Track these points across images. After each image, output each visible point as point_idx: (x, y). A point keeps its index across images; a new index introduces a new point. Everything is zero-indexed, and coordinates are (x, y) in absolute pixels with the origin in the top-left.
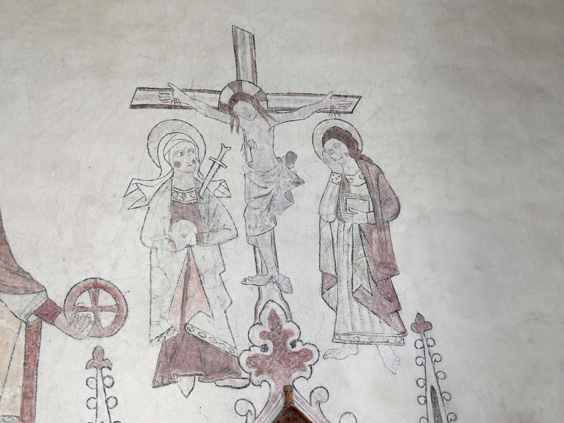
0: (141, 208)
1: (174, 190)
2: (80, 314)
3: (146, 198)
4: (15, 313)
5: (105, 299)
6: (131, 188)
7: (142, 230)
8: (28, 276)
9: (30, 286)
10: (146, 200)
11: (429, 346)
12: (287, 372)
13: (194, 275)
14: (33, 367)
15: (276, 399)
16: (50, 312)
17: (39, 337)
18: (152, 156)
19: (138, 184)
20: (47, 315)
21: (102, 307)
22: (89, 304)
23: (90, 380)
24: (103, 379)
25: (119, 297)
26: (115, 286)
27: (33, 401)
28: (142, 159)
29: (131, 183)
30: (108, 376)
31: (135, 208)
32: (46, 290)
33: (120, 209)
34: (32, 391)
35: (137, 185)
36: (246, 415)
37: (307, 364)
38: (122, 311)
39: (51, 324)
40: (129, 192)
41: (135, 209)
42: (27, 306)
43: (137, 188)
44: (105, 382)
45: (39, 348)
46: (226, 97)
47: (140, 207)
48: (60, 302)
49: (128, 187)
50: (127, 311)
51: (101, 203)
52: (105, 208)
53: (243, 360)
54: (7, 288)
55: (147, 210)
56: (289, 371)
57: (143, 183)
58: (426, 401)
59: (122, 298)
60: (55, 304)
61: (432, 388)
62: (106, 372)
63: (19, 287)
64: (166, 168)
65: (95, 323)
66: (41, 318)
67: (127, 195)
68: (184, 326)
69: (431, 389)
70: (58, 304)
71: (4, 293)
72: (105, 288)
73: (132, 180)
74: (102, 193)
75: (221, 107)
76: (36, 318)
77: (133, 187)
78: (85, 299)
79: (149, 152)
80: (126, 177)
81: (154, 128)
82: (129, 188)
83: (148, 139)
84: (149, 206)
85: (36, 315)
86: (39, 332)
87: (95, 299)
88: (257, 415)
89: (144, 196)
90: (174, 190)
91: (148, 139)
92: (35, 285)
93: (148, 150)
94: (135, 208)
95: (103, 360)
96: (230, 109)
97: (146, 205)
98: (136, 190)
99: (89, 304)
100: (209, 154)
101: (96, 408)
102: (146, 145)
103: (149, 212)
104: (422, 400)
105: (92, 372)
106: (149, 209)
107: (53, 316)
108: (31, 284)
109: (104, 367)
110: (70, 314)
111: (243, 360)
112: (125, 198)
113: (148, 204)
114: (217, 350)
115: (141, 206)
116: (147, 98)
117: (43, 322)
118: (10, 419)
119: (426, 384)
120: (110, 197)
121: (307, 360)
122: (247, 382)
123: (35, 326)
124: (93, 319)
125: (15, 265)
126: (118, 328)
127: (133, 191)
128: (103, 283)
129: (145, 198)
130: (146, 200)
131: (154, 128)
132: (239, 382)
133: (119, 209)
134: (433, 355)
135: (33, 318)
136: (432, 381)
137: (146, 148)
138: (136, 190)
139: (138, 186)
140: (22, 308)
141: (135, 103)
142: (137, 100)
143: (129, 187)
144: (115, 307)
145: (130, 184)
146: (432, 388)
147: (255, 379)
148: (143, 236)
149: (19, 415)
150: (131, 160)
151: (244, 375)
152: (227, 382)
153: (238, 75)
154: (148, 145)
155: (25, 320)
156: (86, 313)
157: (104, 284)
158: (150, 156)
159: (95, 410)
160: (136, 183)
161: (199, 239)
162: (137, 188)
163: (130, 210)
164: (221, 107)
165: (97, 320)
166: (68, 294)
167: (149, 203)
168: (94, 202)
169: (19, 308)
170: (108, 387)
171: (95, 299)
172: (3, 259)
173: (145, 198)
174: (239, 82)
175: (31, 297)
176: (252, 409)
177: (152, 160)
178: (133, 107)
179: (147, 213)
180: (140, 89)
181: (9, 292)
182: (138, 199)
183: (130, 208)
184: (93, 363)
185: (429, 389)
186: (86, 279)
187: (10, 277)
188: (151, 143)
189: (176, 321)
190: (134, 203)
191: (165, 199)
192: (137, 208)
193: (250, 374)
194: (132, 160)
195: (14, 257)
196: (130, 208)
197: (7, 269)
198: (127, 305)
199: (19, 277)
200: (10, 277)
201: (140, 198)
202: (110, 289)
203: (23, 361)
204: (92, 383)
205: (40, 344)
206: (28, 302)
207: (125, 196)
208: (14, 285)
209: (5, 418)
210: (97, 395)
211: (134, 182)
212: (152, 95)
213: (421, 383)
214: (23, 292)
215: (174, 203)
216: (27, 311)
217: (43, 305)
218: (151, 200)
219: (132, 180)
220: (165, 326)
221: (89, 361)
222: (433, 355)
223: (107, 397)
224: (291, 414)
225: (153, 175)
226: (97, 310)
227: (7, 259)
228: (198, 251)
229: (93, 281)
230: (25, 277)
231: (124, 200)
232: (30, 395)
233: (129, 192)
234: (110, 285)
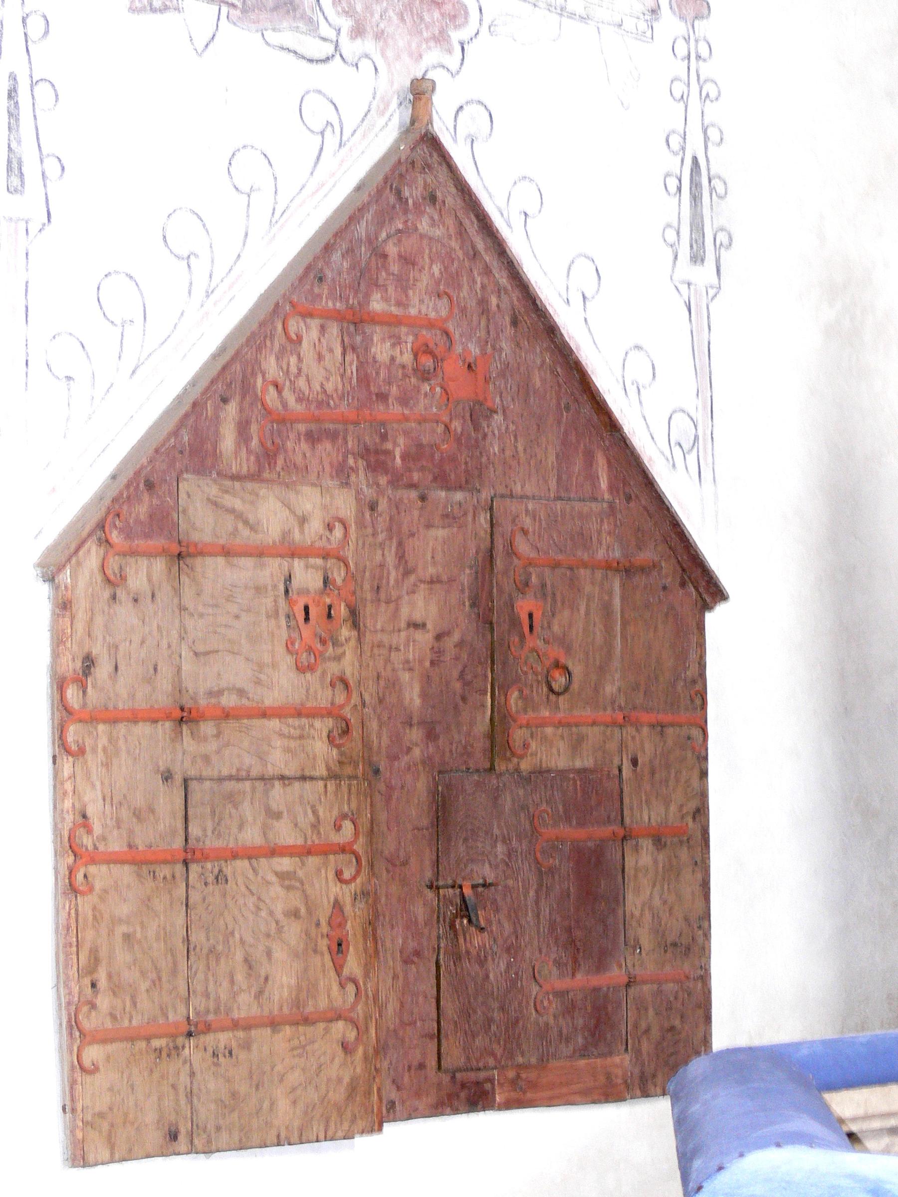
11: (698, 57)
12: (414, 45)
15: (387, 105)
36: (322, 133)
37: (456, 36)
56: (419, 46)
58: (679, 189)
61: (695, 160)
69: (693, 162)
88: (345, 138)
104: (673, 184)
119: (683, 149)
121: (457, 27)
122: (329, 49)
134: (705, 81)
136: (695, 145)
146: (695, 160)
147: (349, 47)
151: (325, 30)
152: (288, 38)
185: (688, 162)
193: (339, 31)
213: (675, 141)
222: (705, 81)
223: (27, 10)
224: (423, 151)
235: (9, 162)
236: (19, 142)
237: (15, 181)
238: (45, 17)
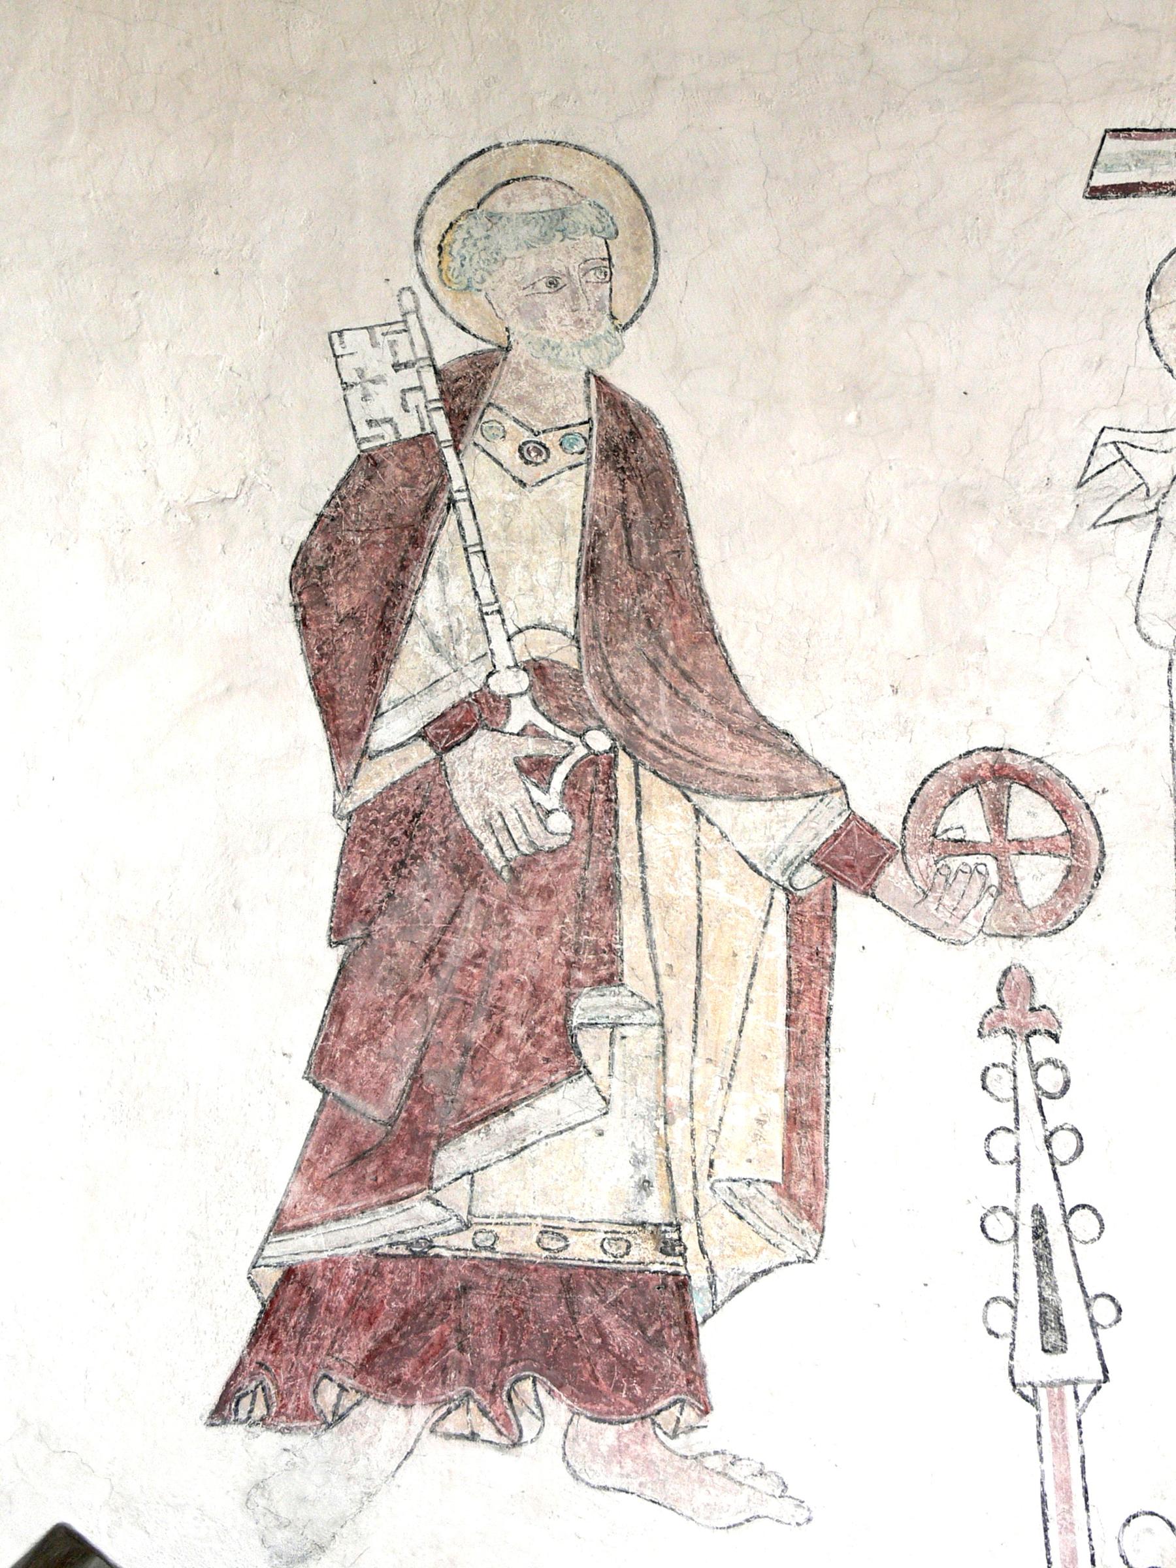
0: (1135, 520)
2: (955, 863)
3: (1148, 490)
4: (755, 861)
6: (1098, 459)
7: (1140, 593)
8: (787, 744)
9: (793, 774)
10: (1148, 495)
14: (814, 1029)
16: (858, 857)
17: (829, 934)
18: (1162, 352)
19: (1120, 445)
20: (851, 867)
21: (1020, 841)
22: (978, 831)
23: (993, 1072)
24: (1035, 1069)
25: (1074, 808)
26: (1060, 775)
27: (819, 1137)
28: (1132, 364)
29: (1099, 444)
30: (1048, 1061)
31: (1115, 522)
32: (844, 786)
33: (1068, 526)
34: (814, 1106)
35: (1118, 449)
38: (1087, 855)
39: (866, 894)
40: (1088, 475)
41: (1113, 526)
42: (787, 838)
43: (1119, 456)
44: (1040, 1081)
45: (831, 969)
47: (1129, 519)
48: (888, 825)
49: (1088, 454)
50: (1103, 854)
51: (1006, 507)
52: (1019, 524)
54: (723, 782)
55: (1153, 527)
57: (1137, 439)
59: (1084, 812)
60: (873, 831)
62: (1042, 1047)
63: (760, 779)
65: (1000, 891)
66: (832, 875)
67: (1087, 481)
70: (884, 831)
71: (715, 796)
72: (1029, 782)
73: (1102, 430)
74: (1007, 475)
76: (818, 874)
77: (1106, 455)
79: (1152, 340)
80: (1081, 422)
81: (1166, 260)
82: (1093, 460)
83: (1149, 296)
84: (1161, 515)
85: (817, 866)
86: (827, 920)
87: (998, 817)
89: (1141, 481)
91: (1149, 296)
92: (809, 772)
93: (1150, 332)
94: (1115, 522)
95: (1032, 1009)
97: (1151, 512)
98: (1114, 463)
99: (978, 831)
101: (1017, 1161)
102: (1143, 316)
103: (1160, 536)
105: (1000, 1047)
106: (1159, 525)
107: (870, 869)
108: (797, 769)
109: (1035, 1033)
110: (921, 862)
112: (1080, 490)
113: (1156, 509)
115: (1135, 516)
116: (1139, 163)
117: (838, 887)
118: (753, 1190)
120: (1034, 488)
123: (816, 899)
124: (994, 879)
125: (746, 709)
126: (1076, 907)
127: (1107, 467)
128: (1021, 764)
129: (1143, 488)
130: (1148, 495)
131: (1166, 260)
133: (1062, 524)
135: (808, 876)
137: (1144, 325)
138: (1114, 463)
139: (1122, 450)
140: (774, 845)
141: (1100, 180)
142: (1108, 169)
143: (1092, 453)
144: (1063, 842)
145: (1095, 444)
148: (1141, 612)
149: (777, 1177)
150: (1095, 364)
154: (1148, 318)
155: (783, 881)
156: (971, 860)
157: (1026, 767)
158: (1158, 353)
159: (1014, 1167)
160: (1114, 443)
162: (1119, 456)
163: (1098, 529)
165: (1008, 883)
166: (913, 800)
167: (1157, 504)
168: (984, 506)
169: (763, 845)
170: (1051, 1097)
171: (998, 817)
172: (708, 689)
173: (1143, 488)
175: (798, 808)
177: (1162, 364)
178: (1096, 193)
179: (1154, 537)
180: (1116, 132)
181: (729, 794)
182: (1122, 493)
183: (1100, 522)
184: (1002, 1019)
186: (969, 753)
187: (731, 745)
188: (1160, 311)
190: (1112, 507)
192: (1121, 520)
194: (1099, 366)
195: (742, 681)
196: (1100, 522)
197: (721, 721)
198: (1099, 834)
199: (760, 747)
200: (731, 745)
201: (1128, 489)
202: (1044, 782)
203: (783, 1011)
204: (1001, 1083)
205: (833, 956)
206: (791, 825)
207: (1080, 485)
208: (746, 771)
209: (735, 1186)
210: (1017, 1120)
211: (1108, 437)
212: (1157, 153)
214: (773, 794)
216: (790, 854)
217: (836, 836)
218: (1164, 496)
219: (1102, 430)
221: (990, 1011)
223: (1050, 1127)
225: (1169, 414)
226: (1006, 850)
227: (721, 689)
229: (989, 757)
230: (777, 746)
231: (1078, 495)
232: (810, 1116)
233: (1092, 470)
234: (1043, 772)
235: (1042, 1314)
236: (1055, 1289)
237: (1053, 1337)
238: (995, 1162)
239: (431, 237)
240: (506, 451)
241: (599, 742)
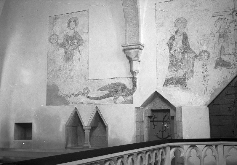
1: (220, 32)
5: (206, 54)
13: (223, 48)
46: (231, 12)
53: (232, 63)
64: (218, 28)
68: (220, 57)
75: (230, 14)
78: (202, 54)
90: (220, 32)
96: (232, 14)
100: (227, 24)
111: (232, 63)
114: (227, 62)
132: (231, 68)
153: (234, 6)
161: (224, 41)
164: (230, 14)
174: (234, 8)
175: (193, 54)
176: (233, 72)
189: (219, 57)
191: (218, 34)
215: (219, 35)
220: (217, 58)
228: (224, 44)
239: (175, 24)
240: (178, 35)
241: (183, 51)
